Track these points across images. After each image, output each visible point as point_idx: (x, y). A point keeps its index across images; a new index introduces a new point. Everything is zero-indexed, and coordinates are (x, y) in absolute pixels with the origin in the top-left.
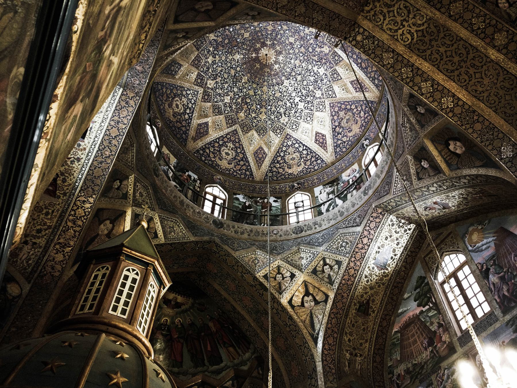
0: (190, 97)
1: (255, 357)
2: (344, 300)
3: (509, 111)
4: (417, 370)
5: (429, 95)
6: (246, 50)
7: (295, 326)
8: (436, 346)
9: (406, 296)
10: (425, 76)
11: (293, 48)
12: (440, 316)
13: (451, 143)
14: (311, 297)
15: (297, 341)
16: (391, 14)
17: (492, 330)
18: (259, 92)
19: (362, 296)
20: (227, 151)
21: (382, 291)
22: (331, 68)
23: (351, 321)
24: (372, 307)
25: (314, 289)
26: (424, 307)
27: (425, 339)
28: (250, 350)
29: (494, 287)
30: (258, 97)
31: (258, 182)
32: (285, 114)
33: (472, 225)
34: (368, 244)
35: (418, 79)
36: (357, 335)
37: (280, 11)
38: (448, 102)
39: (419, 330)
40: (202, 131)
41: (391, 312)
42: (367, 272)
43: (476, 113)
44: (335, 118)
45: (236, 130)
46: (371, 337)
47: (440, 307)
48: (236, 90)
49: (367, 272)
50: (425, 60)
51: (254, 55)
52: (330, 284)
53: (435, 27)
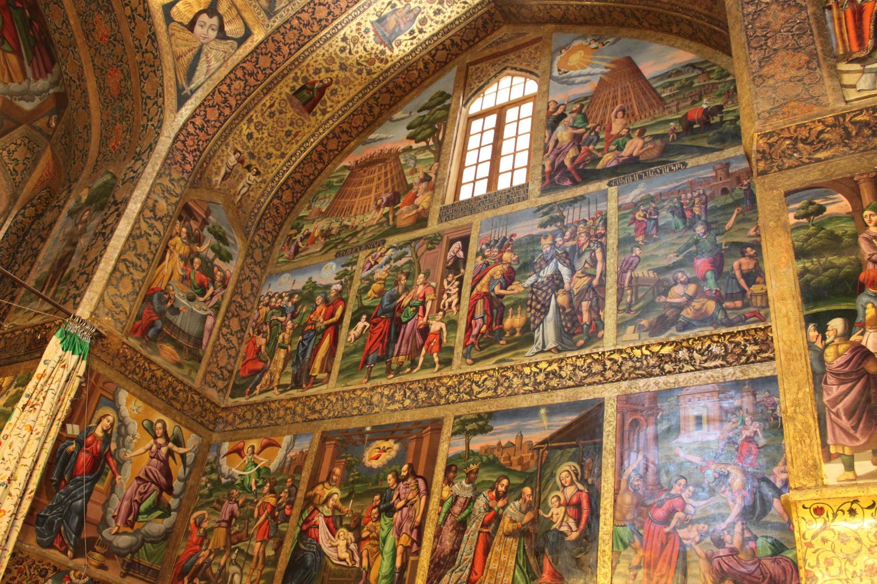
1: (55, 94)
2: (279, 59)
4: (343, 235)
7: (155, 57)
8: (399, 208)
9: (397, 116)
12: (436, 164)
14: (215, 21)
15: (147, 87)
17: (507, 211)
19: (317, 71)
21: (360, 84)
23: (272, 106)
24: (325, 102)
25: (230, 8)
26: (416, 142)
27: (387, 192)
28: (49, 75)
29: (555, 147)
33: (584, 37)
36: (269, 135)
39: (386, 176)
41: (355, 132)
42: (349, 30)
46: (294, 154)
47: (444, 151)
49: (349, 30)
52: (265, 11)
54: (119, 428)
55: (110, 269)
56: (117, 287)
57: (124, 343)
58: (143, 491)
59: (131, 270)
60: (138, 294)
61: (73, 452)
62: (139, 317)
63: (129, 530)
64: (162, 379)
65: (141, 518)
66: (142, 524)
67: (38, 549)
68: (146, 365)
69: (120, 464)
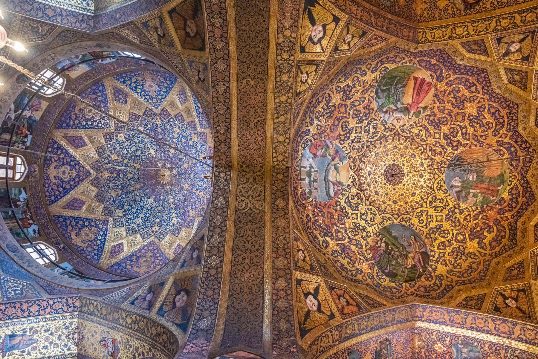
0: (103, 121)
3: (236, 304)
5: (211, 245)
6: (161, 156)
10: (224, 233)
11: (180, 191)
13: (183, 293)
16: (251, 186)
18: (133, 183)
20: (67, 172)
22: (181, 225)
30: (128, 182)
31: (47, 210)
32: (125, 211)
34: (31, 314)
35: (218, 230)
37: (214, 90)
38: (214, 261)
40: (77, 142)
43: (219, 285)
44: (143, 251)
45: (90, 174)
48: (125, 161)
50: (235, 226)
51: (160, 165)
53: (261, 218)
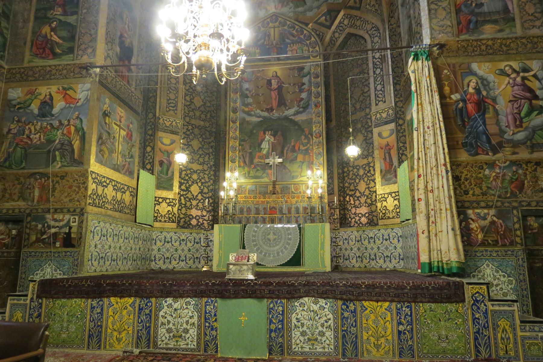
54: (482, 83)
55: (427, 12)
56: (436, 18)
57: (458, 41)
58: (517, 106)
59: (439, 4)
60: (450, 13)
61: (462, 107)
62: (459, 23)
63: (520, 129)
64: (494, 44)
65: (524, 120)
66: (527, 124)
67: (471, 158)
68: (479, 43)
69: (494, 100)
